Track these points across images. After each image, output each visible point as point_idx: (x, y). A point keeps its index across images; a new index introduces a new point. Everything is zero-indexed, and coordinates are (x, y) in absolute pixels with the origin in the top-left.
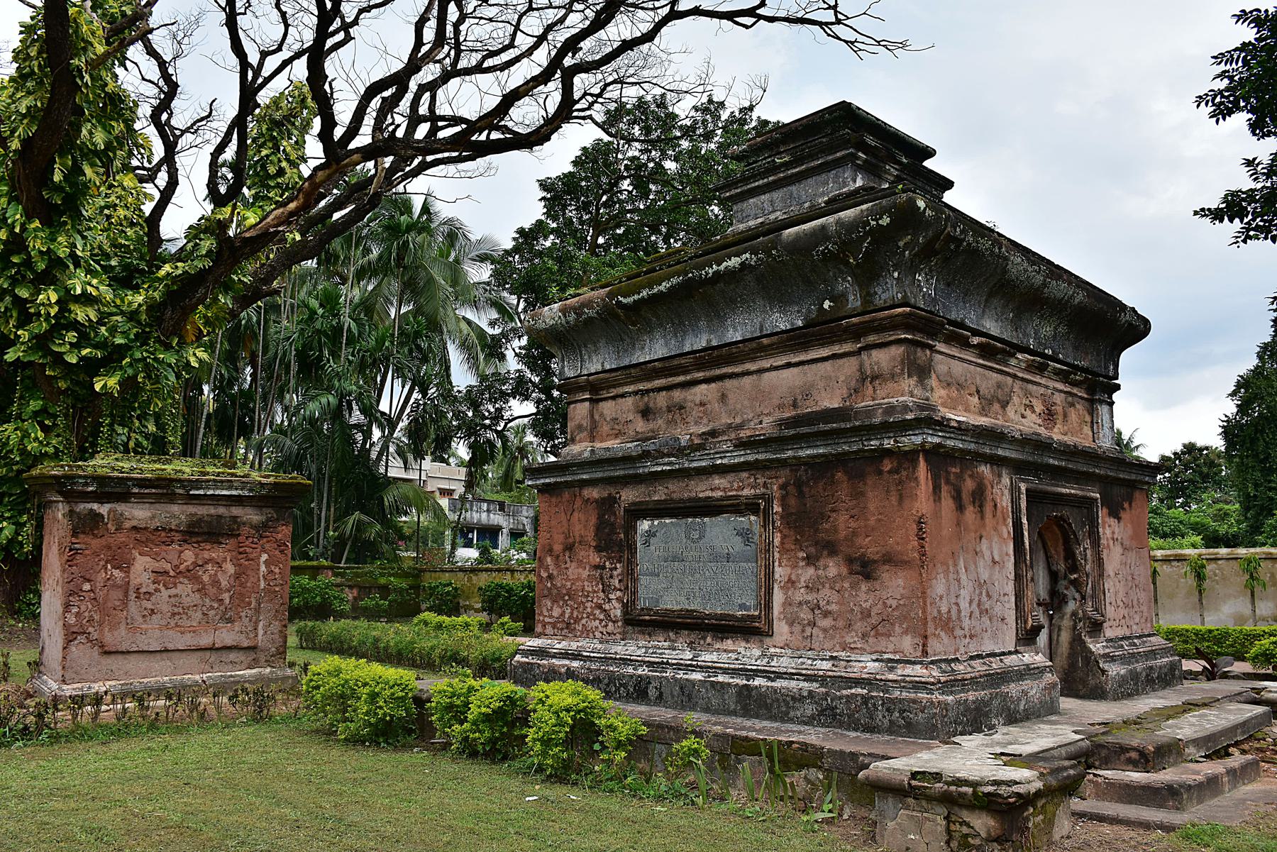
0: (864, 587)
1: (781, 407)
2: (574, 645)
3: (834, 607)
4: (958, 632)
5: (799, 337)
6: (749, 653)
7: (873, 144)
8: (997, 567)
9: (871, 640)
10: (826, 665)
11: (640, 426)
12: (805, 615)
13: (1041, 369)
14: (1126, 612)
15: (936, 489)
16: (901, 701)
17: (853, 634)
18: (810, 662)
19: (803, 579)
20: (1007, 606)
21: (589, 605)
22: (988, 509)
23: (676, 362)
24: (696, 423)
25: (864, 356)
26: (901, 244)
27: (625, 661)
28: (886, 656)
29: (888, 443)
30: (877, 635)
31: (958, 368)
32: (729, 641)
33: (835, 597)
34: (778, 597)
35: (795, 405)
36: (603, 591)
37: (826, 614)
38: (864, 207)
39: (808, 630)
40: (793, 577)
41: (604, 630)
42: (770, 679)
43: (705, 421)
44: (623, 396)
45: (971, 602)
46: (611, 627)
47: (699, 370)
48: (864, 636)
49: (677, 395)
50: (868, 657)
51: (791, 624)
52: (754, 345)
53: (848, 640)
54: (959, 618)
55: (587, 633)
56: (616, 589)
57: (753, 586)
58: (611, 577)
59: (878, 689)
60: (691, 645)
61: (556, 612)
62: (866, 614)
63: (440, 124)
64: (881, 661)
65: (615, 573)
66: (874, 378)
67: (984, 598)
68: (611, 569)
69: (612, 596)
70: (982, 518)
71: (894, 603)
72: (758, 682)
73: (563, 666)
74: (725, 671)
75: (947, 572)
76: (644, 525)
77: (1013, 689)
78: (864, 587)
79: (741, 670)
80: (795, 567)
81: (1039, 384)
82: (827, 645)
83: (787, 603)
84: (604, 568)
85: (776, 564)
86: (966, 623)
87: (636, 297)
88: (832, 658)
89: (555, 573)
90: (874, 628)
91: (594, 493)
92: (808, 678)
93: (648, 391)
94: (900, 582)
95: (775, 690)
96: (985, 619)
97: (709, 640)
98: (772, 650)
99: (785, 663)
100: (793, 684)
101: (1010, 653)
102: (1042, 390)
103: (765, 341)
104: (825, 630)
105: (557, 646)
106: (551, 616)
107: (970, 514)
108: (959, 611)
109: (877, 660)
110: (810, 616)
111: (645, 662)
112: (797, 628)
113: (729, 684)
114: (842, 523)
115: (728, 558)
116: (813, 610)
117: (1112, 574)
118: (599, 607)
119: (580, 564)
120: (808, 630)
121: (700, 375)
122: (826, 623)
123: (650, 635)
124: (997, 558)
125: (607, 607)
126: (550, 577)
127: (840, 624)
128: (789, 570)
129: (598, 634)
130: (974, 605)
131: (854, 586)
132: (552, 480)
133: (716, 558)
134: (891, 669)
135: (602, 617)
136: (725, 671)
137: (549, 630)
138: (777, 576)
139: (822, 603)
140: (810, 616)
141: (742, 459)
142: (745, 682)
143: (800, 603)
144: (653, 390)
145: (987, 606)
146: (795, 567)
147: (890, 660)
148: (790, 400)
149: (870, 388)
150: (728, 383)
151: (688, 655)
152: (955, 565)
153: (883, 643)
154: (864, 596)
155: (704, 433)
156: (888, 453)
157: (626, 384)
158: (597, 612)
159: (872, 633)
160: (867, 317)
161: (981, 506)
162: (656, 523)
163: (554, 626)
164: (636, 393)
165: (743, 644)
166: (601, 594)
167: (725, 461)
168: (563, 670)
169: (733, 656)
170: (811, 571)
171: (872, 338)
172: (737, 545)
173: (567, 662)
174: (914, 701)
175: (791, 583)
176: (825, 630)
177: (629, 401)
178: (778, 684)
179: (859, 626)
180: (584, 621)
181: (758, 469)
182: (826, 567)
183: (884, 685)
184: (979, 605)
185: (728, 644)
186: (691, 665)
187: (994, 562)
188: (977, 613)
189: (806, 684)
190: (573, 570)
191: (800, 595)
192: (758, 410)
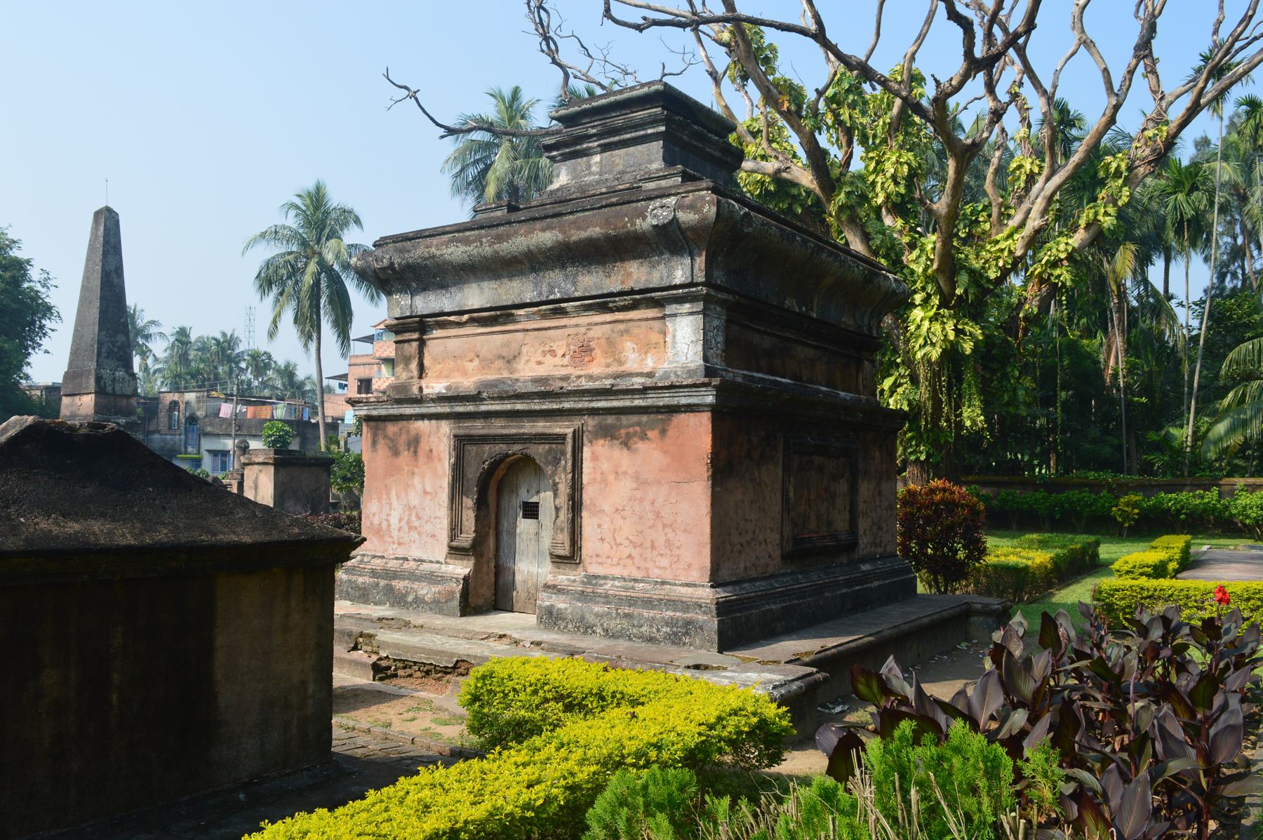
4: (387, 539)
7: (553, 141)
8: (429, 497)
13: (563, 313)
14: (635, 553)
15: (374, 443)
20: (438, 526)
22: (421, 453)
31: (453, 344)
45: (401, 520)
54: (389, 530)
63: (1021, 41)
67: (414, 518)
70: (416, 460)
75: (380, 500)
77: (399, 585)
81: (564, 327)
86: (395, 534)
96: (414, 535)
101: (438, 562)
102: (570, 331)
107: (405, 455)
108: (389, 525)
117: (607, 508)
124: (428, 489)
130: (403, 523)
145: (416, 524)
152: (388, 493)
161: (415, 452)
184: (408, 523)
187: (426, 493)
188: (406, 528)
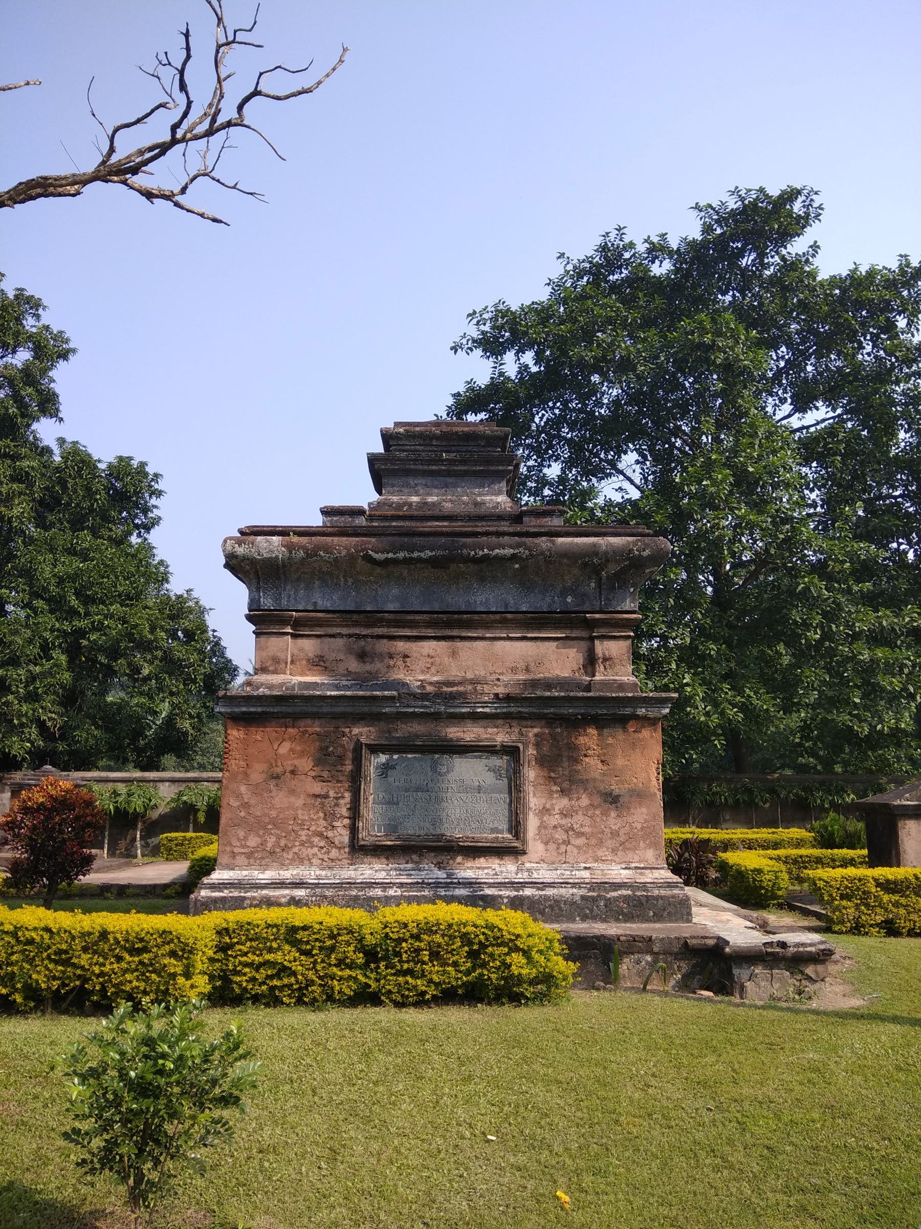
0: (613, 814)
1: (514, 670)
2: (287, 874)
3: (587, 830)
5: (540, 619)
6: (507, 869)
9: (619, 853)
10: (586, 874)
11: (354, 665)
12: (560, 835)
16: (661, 897)
17: (605, 849)
18: (568, 873)
19: (557, 808)
21: (304, 833)
23: (409, 617)
24: (422, 672)
25: (597, 642)
26: (647, 571)
27: (371, 885)
28: (633, 865)
29: (641, 711)
30: (625, 849)
32: (482, 860)
33: (587, 821)
34: (532, 824)
35: (527, 670)
36: (325, 819)
37: (580, 834)
38: (630, 539)
39: (563, 848)
40: (548, 806)
41: (325, 857)
42: (539, 889)
43: (433, 670)
44: (333, 636)
46: (334, 853)
47: (428, 627)
48: (614, 851)
49: (401, 645)
50: (619, 867)
51: (546, 843)
52: (498, 616)
53: (600, 853)
55: (300, 860)
56: (342, 817)
57: (506, 812)
58: (337, 805)
59: (638, 888)
60: (440, 866)
61: (253, 841)
62: (615, 834)
64: (629, 868)
65: (342, 802)
66: (605, 659)
68: (337, 798)
69: (335, 824)
71: (639, 826)
72: (528, 892)
73: (284, 897)
74: (491, 885)
76: (383, 758)
78: (613, 814)
79: (508, 883)
80: (550, 796)
82: (581, 858)
83: (542, 826)
84: (326, 796)
85: (531, 795)
87: (390, 555)
88: (586, 868)
89: (253, 802)
90: (622, 844)
91: (316, 728)
92: (574, 885)
93: (365, 636)
94: (644, 810)
95: (547, 898)
97: (459, 859)
98: (528, 865)
99: (544, 874)
100: (563, 891)
103: (509, 616)
104: (578, 848)
105: (261, 876)
106: (243, 846)
109: (626, 868)
110: (565, 837)
111: (394, 884)
112: (552, 846)
113: (500, 896)
114: (592, 765)
115: (479, 789)
116: (567, 832)
118: (320, 835)
119: (292, 792)
120: (563, 848)
121: (430, 632)
122: (581, 841)
123: (387, 858)
125: (330, 834)
126: (246, 806)
127: (593, 841)
128: (543, 801)
129: (314, 861)
131: (605, 813)
132: (259, 710)
133: (467, 790)
134: (641, 874)
135: (322, 844)
136: (491, 885)
137: (241, 860)
138: (532, 805)
139: (575, 826)
140: (565, 837)
141: (505, 710)
142: (516, 893)
143: (555, 827)
144: (372, 637)
146: (550, 796)
147: (636, 868)
148: (521, 665)
149: (602, 666)
150: (459, 644)
151: (441, 874)
153: (630, 855)
154: (613, 821)
155: (437, 682)
156: (636, 717)
157: (337, 626)
158: (316, 839)
159: (621, 848)
160: (608, 616)
162: (395, 757)
163: (249, 855)
164: (350, 636)
165: (497, 861)
166: (323, 823)
167: (487, 710)
168: (283, 900)
169: (490, 871)
170: (564, 802)
171: (603, 631)
172: (489, 779)
173: (287, 892)
174: (673, 897)
175: (545, 811)
176: (578, 848)
177: (340, 642)
178: (550, 892)
179: (609, 843)
180: (296, 850)
181: (513, 718)
182: (578, 799)
183: (644, 886)
185: (482, 862)
186: (451, 883)
189: (575, 890)
190: (280, 799)
191: (554, 820)
192: (491, 669)
